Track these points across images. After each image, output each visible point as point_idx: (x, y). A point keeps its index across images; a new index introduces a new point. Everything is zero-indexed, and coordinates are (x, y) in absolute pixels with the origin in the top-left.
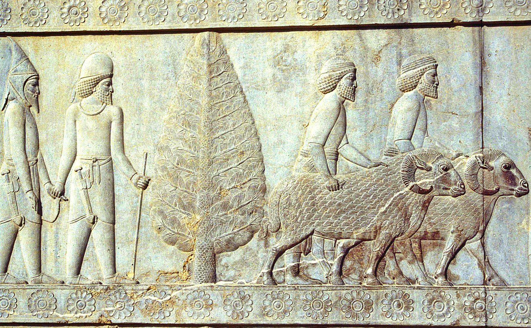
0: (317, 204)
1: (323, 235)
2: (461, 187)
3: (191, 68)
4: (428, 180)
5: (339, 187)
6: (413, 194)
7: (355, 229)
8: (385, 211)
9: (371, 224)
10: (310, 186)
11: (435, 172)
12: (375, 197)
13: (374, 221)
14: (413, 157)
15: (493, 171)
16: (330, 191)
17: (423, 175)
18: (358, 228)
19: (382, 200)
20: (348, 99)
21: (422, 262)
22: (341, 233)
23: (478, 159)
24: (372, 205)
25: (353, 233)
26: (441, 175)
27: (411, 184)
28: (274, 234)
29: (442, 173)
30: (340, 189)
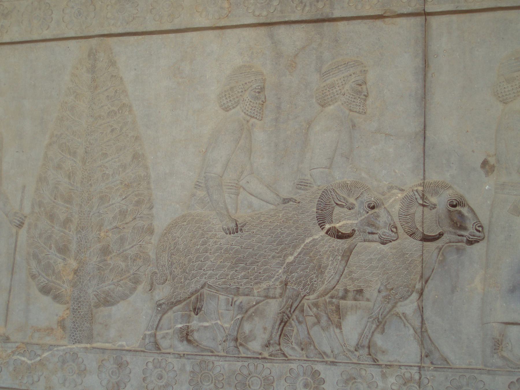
0: (211, 250)
1: (217, 291)
2: (392, 231)
3: (75, 84)
4: (349, 222)
5: (237, 229)
6: (330, 239)
7: (256, 283)
8: (294, 261)
9: (276, 277)
10: (203, 227)
11: (359, 211)
12: (281, 243)
13: (280, 274)
14: (331, 192)
15: (435, 210)
16: (227, 234)
17: (343, 214)
18: (259, 283)
19: (290, 246)
20: (253, 117)
21: (341, 329)
22: (239, 288)
23: (416, 193)
24: (278, 253)
25: (253, 288)
26: (366, 215)
27: (327, 226)
29: (368, 212)
30: (239, 232)
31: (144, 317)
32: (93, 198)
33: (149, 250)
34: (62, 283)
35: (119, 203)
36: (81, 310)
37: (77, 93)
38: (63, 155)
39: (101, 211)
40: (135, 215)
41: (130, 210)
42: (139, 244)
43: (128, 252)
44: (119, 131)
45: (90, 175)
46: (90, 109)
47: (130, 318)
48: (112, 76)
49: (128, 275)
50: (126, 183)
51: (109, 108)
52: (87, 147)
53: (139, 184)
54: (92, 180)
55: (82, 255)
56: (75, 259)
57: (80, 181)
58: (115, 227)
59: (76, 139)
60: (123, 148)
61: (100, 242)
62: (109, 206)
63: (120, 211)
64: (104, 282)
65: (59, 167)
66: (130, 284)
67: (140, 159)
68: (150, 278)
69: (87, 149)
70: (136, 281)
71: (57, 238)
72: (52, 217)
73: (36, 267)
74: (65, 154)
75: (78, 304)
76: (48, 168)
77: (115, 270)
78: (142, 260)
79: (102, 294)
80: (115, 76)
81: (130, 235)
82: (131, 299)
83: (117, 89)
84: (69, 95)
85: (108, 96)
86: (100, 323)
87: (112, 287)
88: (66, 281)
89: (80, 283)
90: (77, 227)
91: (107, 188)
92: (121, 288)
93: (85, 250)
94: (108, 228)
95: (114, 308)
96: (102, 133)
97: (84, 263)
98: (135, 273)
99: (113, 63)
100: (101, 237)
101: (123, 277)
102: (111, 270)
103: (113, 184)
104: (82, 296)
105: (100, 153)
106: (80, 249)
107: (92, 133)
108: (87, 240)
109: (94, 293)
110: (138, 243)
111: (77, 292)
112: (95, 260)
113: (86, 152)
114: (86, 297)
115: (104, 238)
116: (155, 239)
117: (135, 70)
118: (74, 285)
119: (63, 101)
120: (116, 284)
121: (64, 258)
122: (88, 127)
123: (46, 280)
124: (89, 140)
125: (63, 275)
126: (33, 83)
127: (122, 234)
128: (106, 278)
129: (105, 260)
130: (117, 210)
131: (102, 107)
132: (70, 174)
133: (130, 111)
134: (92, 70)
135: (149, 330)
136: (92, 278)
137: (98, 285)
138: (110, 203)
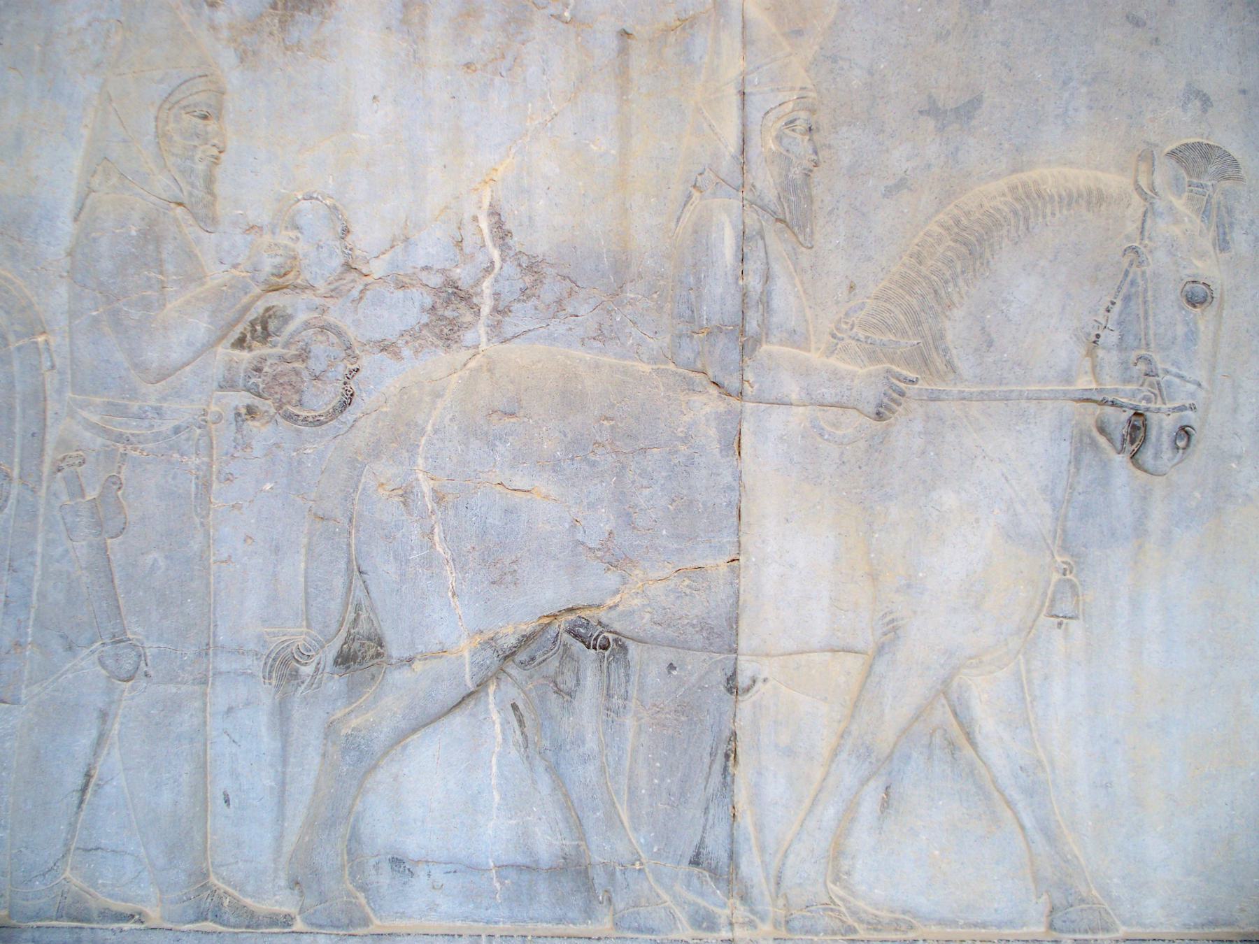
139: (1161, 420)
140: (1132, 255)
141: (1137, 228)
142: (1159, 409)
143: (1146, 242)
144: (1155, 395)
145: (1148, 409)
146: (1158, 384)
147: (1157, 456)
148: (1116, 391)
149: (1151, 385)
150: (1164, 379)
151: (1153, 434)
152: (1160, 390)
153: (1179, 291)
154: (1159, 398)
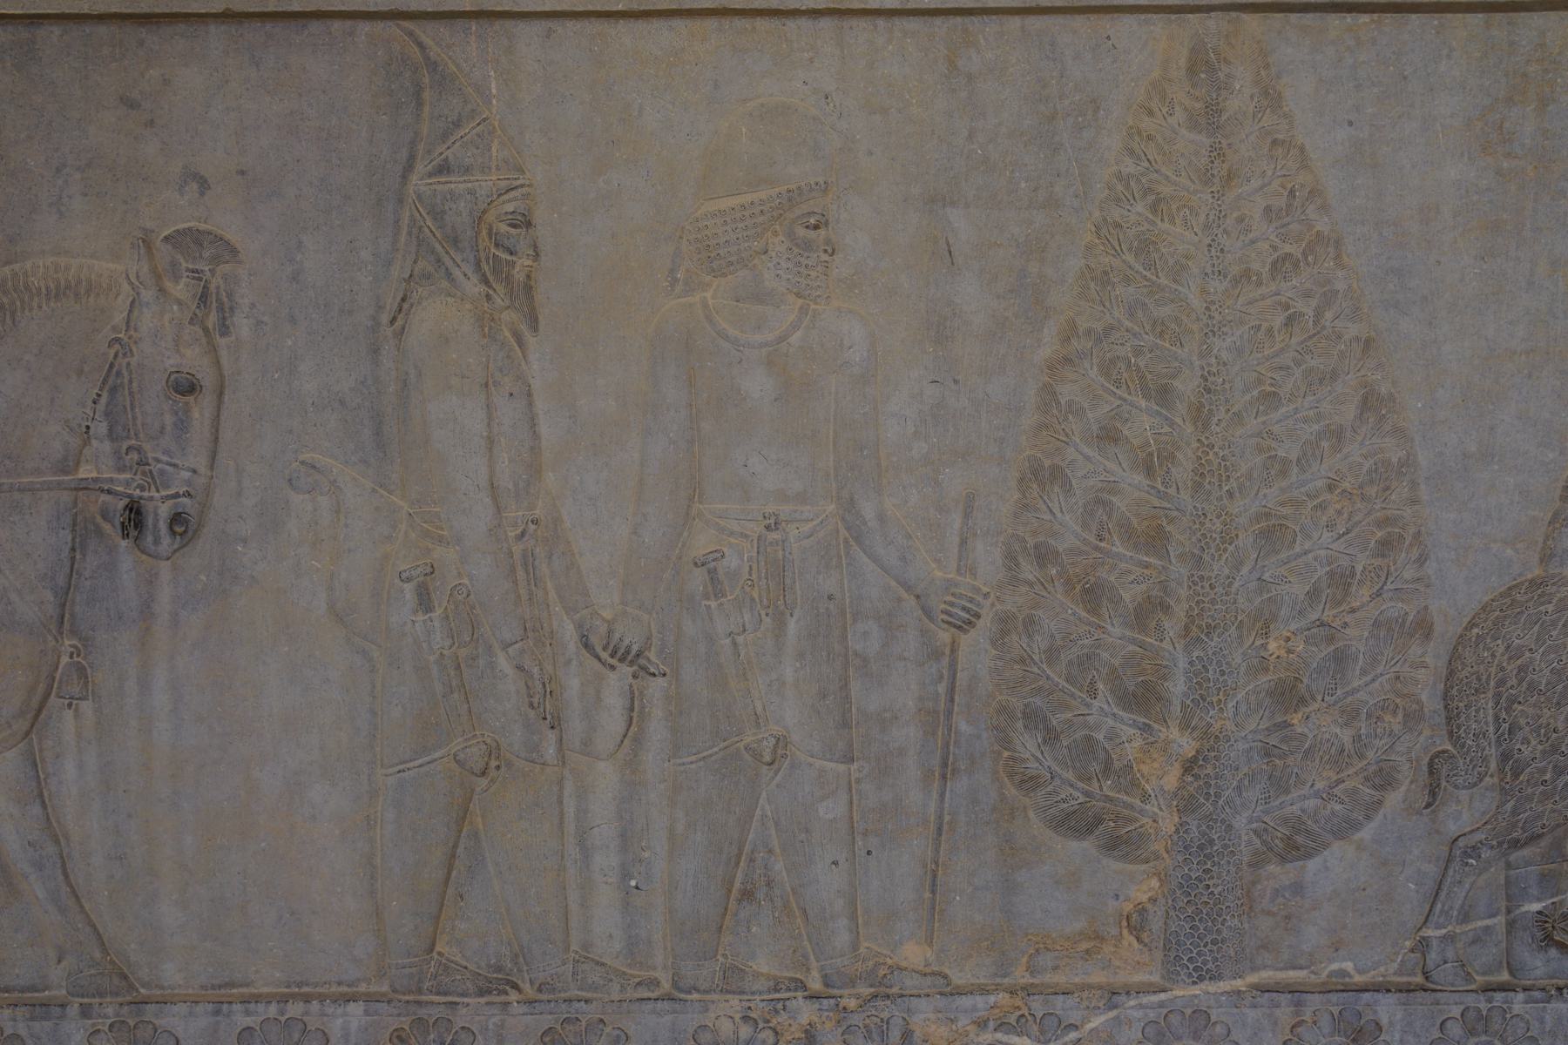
3: (1146, 164)
28: (1464, 794)
31: (1413, 887)
32: (1237, 536)
33: (1420, 686)
34: (1140, 803)
35: (1328, 548)
36: (1215, 881)
37: (1158, 194)
38: (1120, 398)
39: (1266, 576)
40: (1380, 585)
41: (1361, 568)
42: (1392, 670)
43: (1362, 695)
44: (1311, 323)
45: (1228, 464)
46: (1213, 250)
47: (1364, 890)
48: (1275, 142)
49: (1360, 765)
50: (1346, 485)
51: (1275, 248)
52: (1208, 372)
53: (1388, 488)
54: (1232, 480)
55: (1211, 713)
56: (1185, 725)
57: (1190, 484)
58: (1318, 623)
59: (1167, 345)
60: (1328, 376)
61: (1266, 670)
62: (1296, 559)
63: (1331, 574)
64: (1287, 792)
65: (1108, 436)
66: (1368, 791)
67: (1383, 412)
68: (1425, 768)
69: (1211, 379)
70: (1384, 779)
71: (1117, 662)
72: (1093, 596)
73: (1040, 757)
74: (1130, 394)
75: (1205, 863)
76: (1064, 439)
77: (1321, 753)
78: (1400, 717)
79: (1280, 829)
80: (1284, 142)
81: (1366, 645)
82: (1366, 834)
83: (1294, 186)
84: (1128, 200)
85: (1268, 209)
86: (1269, 913)
87: (1311, 803)
88: (1153, 795)
89: (1207, 800)
90: (1187, 629)
91: (1282, 504)
92: (1338, 807)
93: (1221, 697)
94: (1293, 627)
95: (1313, 865)
96: (1259, 328)
97: (1219, 737)
98: (1384, 757)
99: (1270, 97)
100: (1271, 655)
101: (1346, 773)
102: (1307, 753)
103: (1303, 490)
104: (1215, 837)
105: (1255, 393)
106: (1201, 696)
107: (1224, 329)
108: (1224, 667)
109: (1254, 825)
110: (1390, 668)
111: (1199, 826)
112: (1253, 727)
113: (1209, 391)
114: (1229, 840)
115: (1278, 657)
116: (1434, 655)
117: (1350, 123)
118: (1186, 805)
119: (1105, 220)
120: (1324, 796)
121: (1144, 724)
122: (1207, 308)
123: (1079, 794)
124: (1215, 351)
125: (1143, 777)
126: (979, 151)
127: (1341, 644)
128: (1292, 782)
129: (1287, 725)
130: (1322, 571)
131: (1253, 242)
132: (1152, 461)
133: (1338, 257)
134: (1210, 118)
135: (1438, 927)
136: (1246, 783)
137: (1267, 801)
138: (1297, 549)
139: (156, 508)
140: (117, 346)
141: (123, 318)
142: (152, 497)
143: (132, 332)
144: (148, 483)
145: (141, 498)
146: (151, 471)
147: (157, 542)
148: (111, 480)
149: (144, 473)
150: (155, 468)
151: (150, 521)
152: (153, 478)
153: (164, 382)
154: (153, 486)
